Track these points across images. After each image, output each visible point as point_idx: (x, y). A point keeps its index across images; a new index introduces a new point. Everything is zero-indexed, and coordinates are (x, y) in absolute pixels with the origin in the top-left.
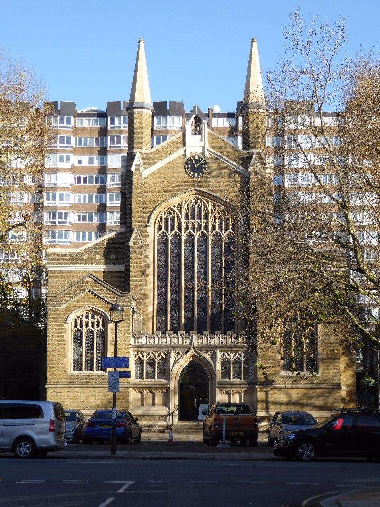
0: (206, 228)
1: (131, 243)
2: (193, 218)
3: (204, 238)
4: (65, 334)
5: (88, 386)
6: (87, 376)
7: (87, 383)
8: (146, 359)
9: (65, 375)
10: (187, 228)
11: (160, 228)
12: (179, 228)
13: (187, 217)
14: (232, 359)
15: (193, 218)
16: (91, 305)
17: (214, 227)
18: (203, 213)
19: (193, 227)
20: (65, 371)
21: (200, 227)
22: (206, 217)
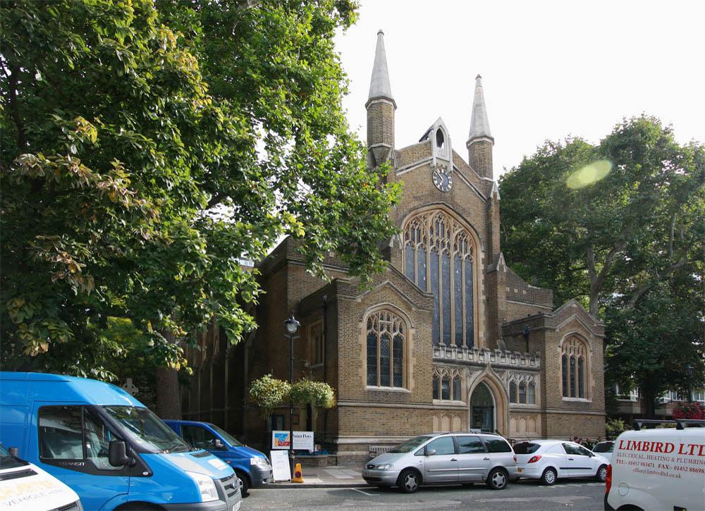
1: (391, 245)
3: (447, 254)
4: (360, 336)
5: (389, 405)
6: (387, 393)
7: (387, 402)
8: (442, 376)
15: (438, 234)
20: (361, 385)
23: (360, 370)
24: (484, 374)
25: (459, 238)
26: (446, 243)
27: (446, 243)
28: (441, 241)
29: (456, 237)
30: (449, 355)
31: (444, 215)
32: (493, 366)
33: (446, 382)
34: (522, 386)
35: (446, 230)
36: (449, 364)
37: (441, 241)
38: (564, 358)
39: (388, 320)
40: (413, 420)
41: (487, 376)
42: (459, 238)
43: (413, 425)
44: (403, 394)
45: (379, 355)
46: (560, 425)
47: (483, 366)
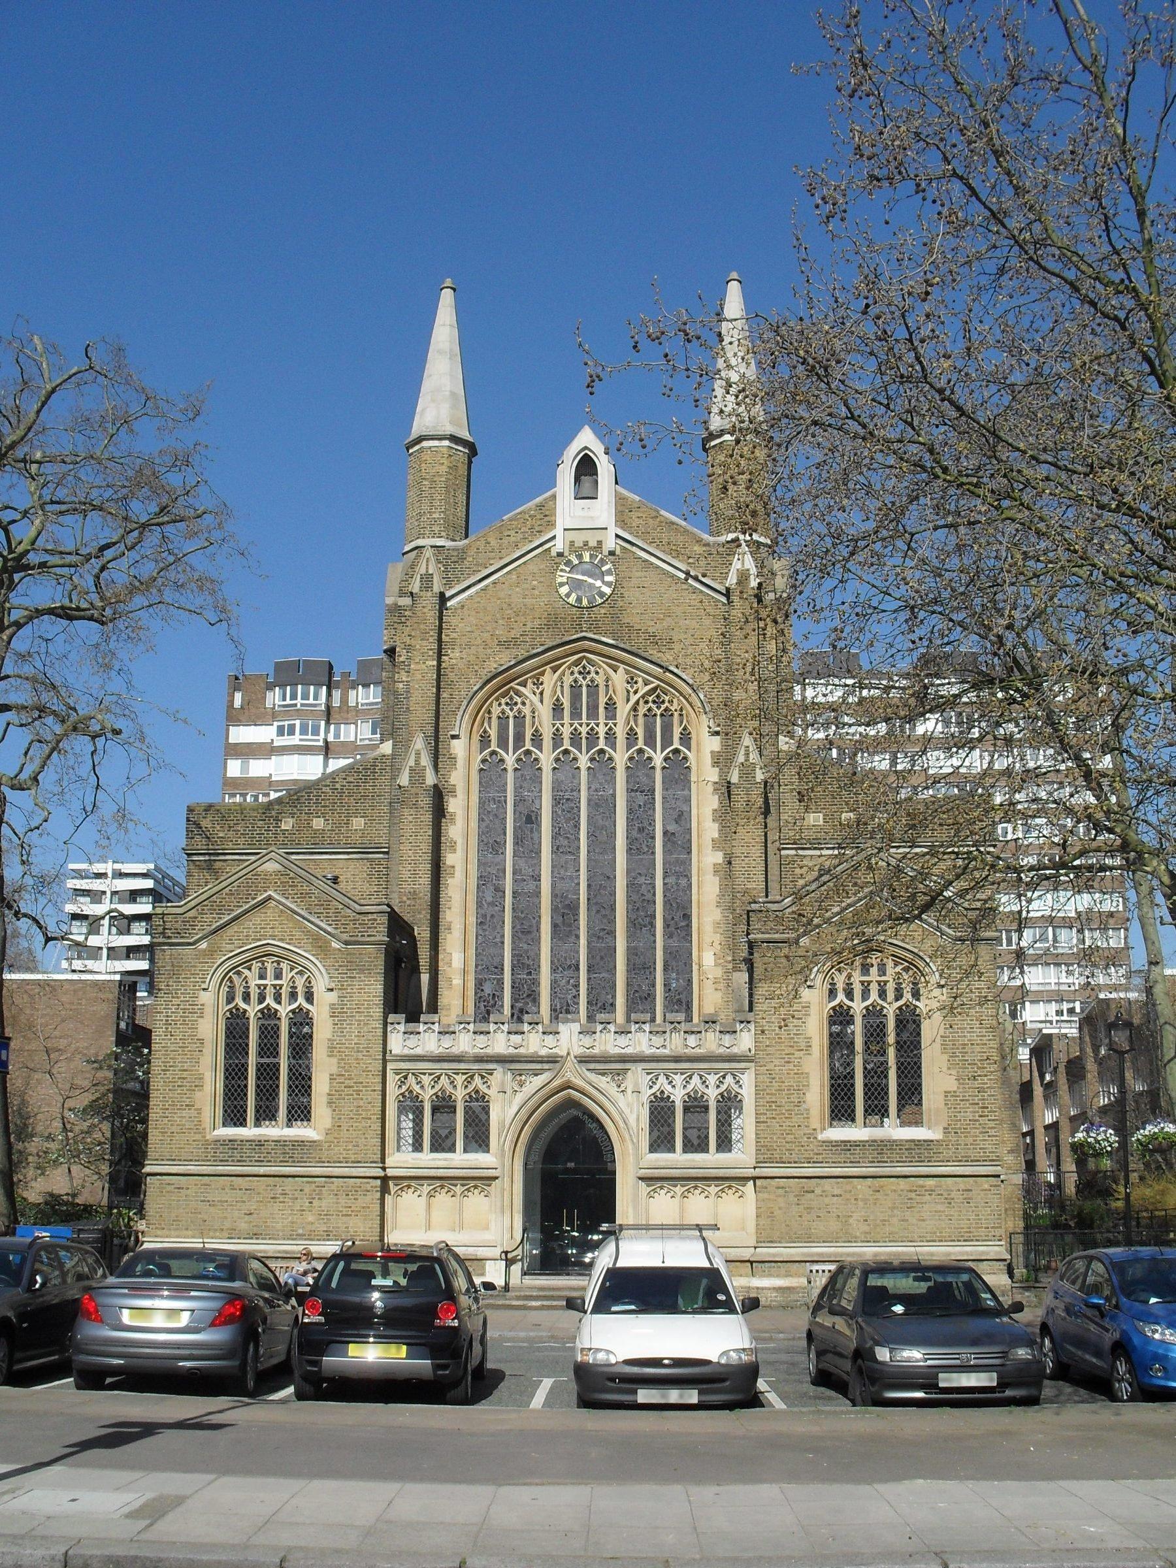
0: (610, 737)
2: (576, 714)
3: (603, 763)
5: (262, 1170)
9: (198, 1137)
10: (557, 738)
11: (485, 740)
12: (537, 739)
13: (557, 709)
14: (678, 1096)
16: (273, 937)
17: (631, 736)
18: (602, 700)
19: (575, 738)
20: (198, 1127)
21: (592, 737)
22: (611, 707)
23: (198, 1094)
24: (557, 1083)
25: (642, 709)
26: (602, 735)
27: (602, 735)
28: (584, 730)
29: (635, 709)
30: (447, 1041)
31: (590, 661)
32: (583, 1060)
33: (444, 1106)
34: (695, 1106)
35: (602, 700)
36: (446, 1065)
37: (584, 730)
38: (840, 1017)
39: (278, 976)
40: (324, 1203)
41: (567, 1086)
42: (642, 709)
43: (324, 1215)
44: (300, 1143)
45: (252, 1060)
46: (809, 1209)
47: (553, 1060)
